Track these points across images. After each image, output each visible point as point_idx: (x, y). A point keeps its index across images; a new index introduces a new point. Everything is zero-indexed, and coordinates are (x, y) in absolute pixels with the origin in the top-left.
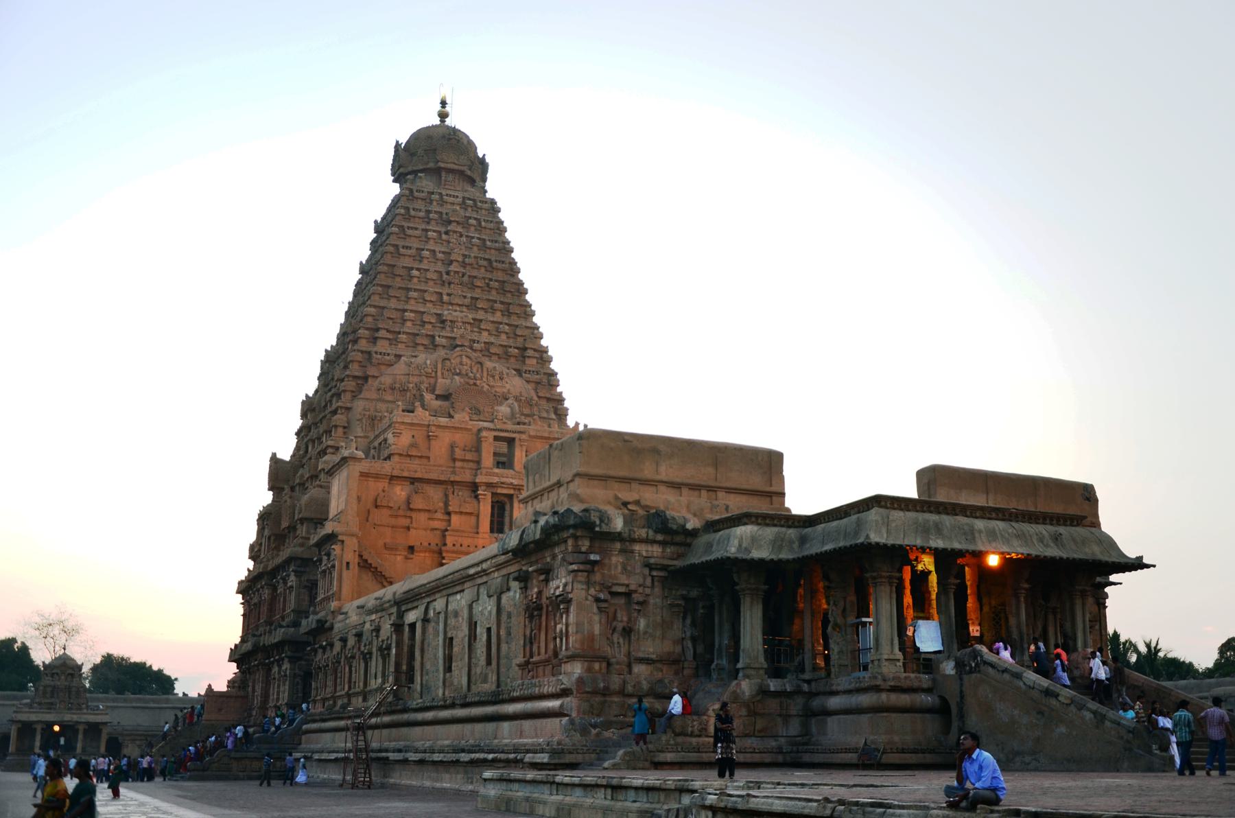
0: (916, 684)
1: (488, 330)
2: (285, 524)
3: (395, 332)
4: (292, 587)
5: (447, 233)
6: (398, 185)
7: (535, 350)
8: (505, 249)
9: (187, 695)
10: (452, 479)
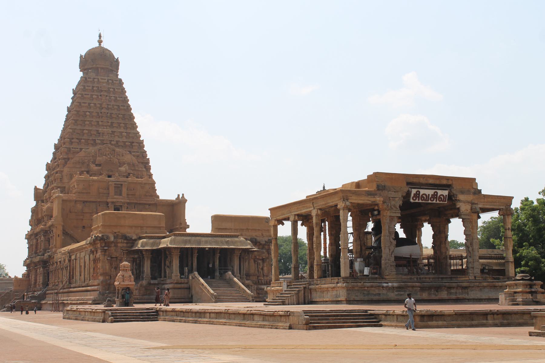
0: (183, 282)
1: (118, 136)
2: (40, 216)
3: (80, 139)
4: (42, 241)
5: (101, 95)
6: (82, 72)
7: (137, 143)
8: (125, 100)
9: (11, 277)
10: (99, 201)
